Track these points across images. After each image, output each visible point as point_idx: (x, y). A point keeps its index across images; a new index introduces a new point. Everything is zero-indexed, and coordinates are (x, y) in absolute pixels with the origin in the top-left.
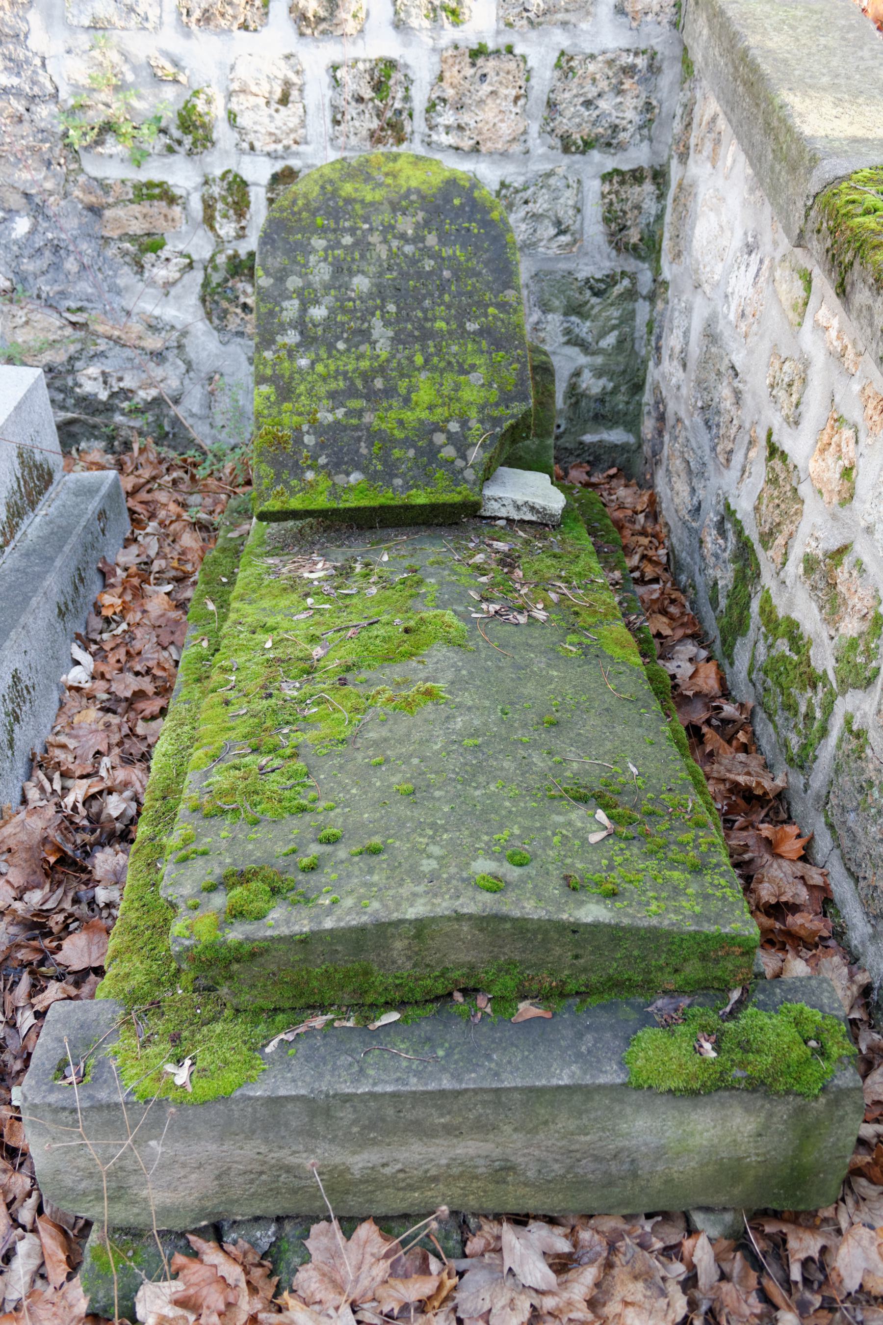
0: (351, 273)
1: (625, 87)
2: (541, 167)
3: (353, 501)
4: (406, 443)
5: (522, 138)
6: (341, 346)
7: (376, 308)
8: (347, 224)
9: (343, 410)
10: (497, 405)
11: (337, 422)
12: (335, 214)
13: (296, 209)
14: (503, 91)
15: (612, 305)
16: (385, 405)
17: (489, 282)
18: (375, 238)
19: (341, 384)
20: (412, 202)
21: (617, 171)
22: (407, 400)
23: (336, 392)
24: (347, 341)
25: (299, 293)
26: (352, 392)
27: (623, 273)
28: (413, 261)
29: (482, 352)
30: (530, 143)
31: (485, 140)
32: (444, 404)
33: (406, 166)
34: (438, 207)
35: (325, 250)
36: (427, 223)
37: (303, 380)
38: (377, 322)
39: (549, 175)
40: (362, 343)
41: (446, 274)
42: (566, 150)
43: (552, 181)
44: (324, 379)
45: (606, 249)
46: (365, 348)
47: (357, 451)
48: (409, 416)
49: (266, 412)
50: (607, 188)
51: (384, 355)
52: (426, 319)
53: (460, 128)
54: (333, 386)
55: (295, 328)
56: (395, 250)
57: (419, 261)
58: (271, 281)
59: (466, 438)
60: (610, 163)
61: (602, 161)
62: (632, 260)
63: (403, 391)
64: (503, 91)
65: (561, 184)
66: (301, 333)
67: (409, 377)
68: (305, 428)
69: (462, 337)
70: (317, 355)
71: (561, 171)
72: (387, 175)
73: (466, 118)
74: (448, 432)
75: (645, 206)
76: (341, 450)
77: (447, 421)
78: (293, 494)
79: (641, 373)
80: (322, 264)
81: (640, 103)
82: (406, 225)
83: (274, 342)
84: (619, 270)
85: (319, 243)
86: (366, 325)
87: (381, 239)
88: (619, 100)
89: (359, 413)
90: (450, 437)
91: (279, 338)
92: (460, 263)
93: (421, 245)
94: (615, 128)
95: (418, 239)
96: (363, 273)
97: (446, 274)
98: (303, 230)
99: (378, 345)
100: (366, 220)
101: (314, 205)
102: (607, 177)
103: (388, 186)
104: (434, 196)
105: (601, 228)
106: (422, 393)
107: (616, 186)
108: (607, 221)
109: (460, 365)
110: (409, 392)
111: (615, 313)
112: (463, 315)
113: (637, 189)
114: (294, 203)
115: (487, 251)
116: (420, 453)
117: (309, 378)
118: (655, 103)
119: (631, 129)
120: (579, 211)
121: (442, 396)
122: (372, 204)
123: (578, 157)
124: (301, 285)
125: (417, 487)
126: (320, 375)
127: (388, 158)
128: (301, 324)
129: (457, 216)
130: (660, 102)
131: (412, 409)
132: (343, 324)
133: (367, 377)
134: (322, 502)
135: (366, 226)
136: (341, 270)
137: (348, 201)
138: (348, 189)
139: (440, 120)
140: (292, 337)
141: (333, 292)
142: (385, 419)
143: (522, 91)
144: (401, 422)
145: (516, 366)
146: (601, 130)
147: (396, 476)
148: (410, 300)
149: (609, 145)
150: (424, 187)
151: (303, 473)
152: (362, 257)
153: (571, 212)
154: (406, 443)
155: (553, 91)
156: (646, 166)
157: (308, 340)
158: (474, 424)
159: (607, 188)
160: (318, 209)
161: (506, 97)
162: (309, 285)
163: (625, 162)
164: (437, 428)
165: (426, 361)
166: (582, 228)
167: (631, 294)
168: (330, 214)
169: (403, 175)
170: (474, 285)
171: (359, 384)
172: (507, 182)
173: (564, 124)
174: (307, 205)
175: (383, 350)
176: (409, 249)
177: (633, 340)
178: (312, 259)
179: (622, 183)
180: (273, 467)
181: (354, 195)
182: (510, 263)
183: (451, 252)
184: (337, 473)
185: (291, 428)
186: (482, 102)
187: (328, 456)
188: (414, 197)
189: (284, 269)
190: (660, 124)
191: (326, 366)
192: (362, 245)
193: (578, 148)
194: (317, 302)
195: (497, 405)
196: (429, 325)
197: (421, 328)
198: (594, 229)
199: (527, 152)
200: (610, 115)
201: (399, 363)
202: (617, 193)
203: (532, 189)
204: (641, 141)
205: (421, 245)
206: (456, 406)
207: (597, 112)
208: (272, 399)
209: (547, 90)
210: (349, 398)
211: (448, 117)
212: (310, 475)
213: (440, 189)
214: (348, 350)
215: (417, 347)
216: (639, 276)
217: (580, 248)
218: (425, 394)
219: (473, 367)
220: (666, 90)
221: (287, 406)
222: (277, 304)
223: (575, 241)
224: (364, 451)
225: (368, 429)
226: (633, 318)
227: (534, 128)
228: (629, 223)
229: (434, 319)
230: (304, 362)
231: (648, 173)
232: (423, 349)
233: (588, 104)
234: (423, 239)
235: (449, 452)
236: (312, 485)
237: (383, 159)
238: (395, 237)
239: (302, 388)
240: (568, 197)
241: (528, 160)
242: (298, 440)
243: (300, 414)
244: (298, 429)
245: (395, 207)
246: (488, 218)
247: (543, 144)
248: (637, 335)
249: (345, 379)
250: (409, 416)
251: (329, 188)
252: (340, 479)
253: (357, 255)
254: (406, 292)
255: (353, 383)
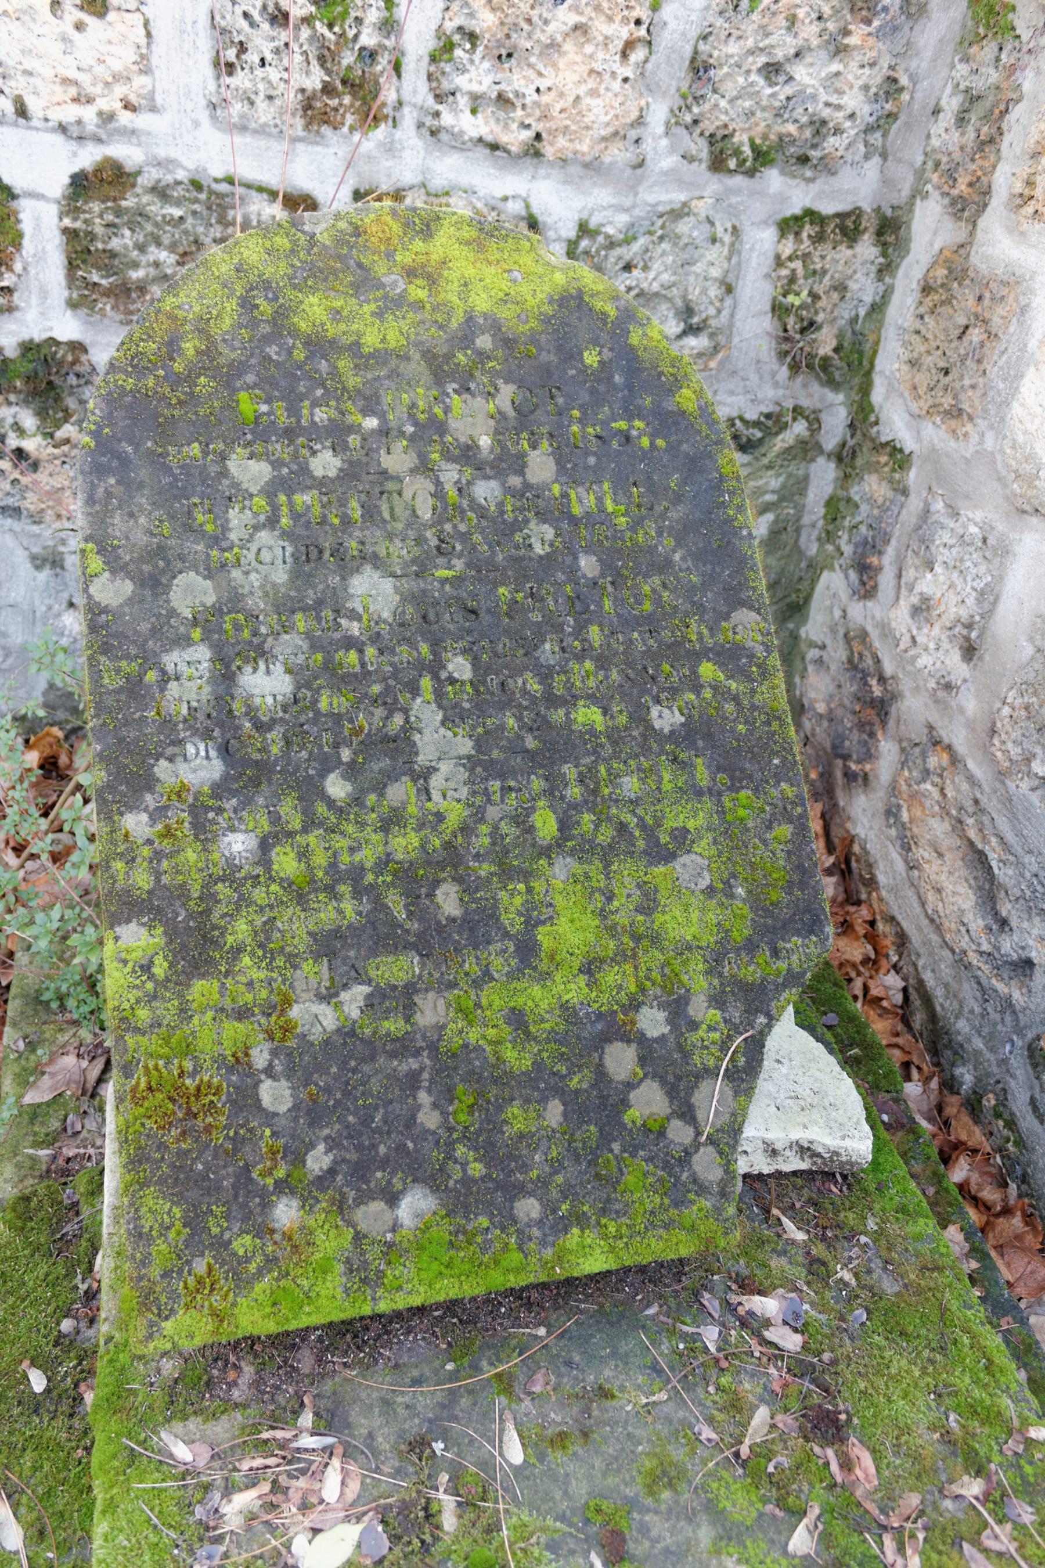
0: (347, 564)
1: (852, 40)
2: (664, 197)
3: (413, 1287)
4: (540, 1084)
5: (633, 134)
6: (337, 787)
7: (421, 667)
8: (321, 415)
9: (361, 990)
10: (750, 947)
11: (348, 1032)
12: (285, 384)
13: (178, 367)
14: (601, 27)
15: (769, 467)
16: (470, 965)
17: (692, 588)
18: (397, 459)
19: (348, 907)
20: (483, 356)
21: (810, 214)
22: (527, 950)
23: (336, 934)
24: (352, 771)
25: (208, 622)
26: (380, 935)
27: (798, 411)
28: (504, 529)
29: (699, 793)
30: (647, 146)
31: (554, 132)
32: (621, 957)
33: (455, 250)
34: (546, 370)
35: (270, 492)
36: (524, 415)
37: (243, 901)
38: (425, 711)
39: (679, 213)
40: (390, 776)
41: (588, 564)
42: (717, 164)
43: (683, 227)
44: (300, 893)
45: (770, 361)
46: (400, 791)
47: (411, 1121)
48: (538, 998)
49: (143, 1014)
50: (788, 248)
51: (455, 814)
52: (551, 700)
53: (502, 100)
54: (327, 915)
55: (206, 735)
56: (452, 493)
57: (516, 526)
58: (128, 587)
59: (686, 1055)
60: (797, 195)
61: (785, 191)
62: (815, 387)
63: (511, 920)
64: (601, 27)
65: (699, 234)
66: (225, 751)
67: (526, 875)
68: (260, 1058)
69: (646, 750)
70: (275, 819)
71: (702, 207)
72: (410, 273)
73: (518, 81)
74: (641, 1039)
75: (853, 286)
76: (366, 1121)
77: (634, 1005)
78: (242, 1282)
79: (804, 585)
80: (264, 536)
81: (875, 78)
82: (473, 420)
83: (149, 782)
84: (789, 404)
85: (250, 471)
86: (398, 720)
87: (410, 460)
88: (835, 67)
89: (404, 998)
90: (649, 1054)
91: (162, 769)
92: (617, 535)
93: (515, 481)
94: (820, 127)
95: (507, 463)
96: (376, 561)
97: (588, 564)
98: (203, 431)
99: (436, 782)
100: (370, 405)
101: (228, 355)
102: (789, 226)
103: (418, 306)
104: (533, 339)
105: (767, 323)
106: (563, 925)
107: (806, 245)
108: (779, 310)
109: (650, 832)
110: (531, 924)
111: (774, 482)
112: (641, 684)
113: (844, 252)
114: (172, 347)
115: (678, 499)
116: (577, 1109)
117: (259, 895)
118: (904, 81)
119: (851, 130)
120: (729, 289)
121: (612, 930)
122: (380, 357)
123: (739, 180)
124: (211, 599)
125: (581, 1220)
126: (288, 884)
127: (407, 225)
128: (222, 721)
129: (598, 400)
130: (914, 79)
131: (544, 977)
132: (337, 718)
133: (415, 879)
134: (330, 1301)
135: (371, 423)
136: (319, 555)
137: (319, 345)
138: (314, 310)
139: (461, 81)
140: (199, 766)
141: (300, 622)
142: (474, 1015)
143: (642, 32)
144: (517, 1019)
145: (784, 831)
146: (791, 128)
147: (520, 1190)
148: (504, 644)
149: (804, 160)
150: (506, 313)
151: (267, 1206)
152: (370, 513)
153: (714, 292)
154: (540, 1084)
155: (705, 38)
156: (867, 208)
157: (245, 776)
158: (700, 1008)
159: (788, 248)
160: (239, 369)
161: (607, 40)
162: (233, 600)
163: (829, 197)
164: (615, 1027)
165: (565, 825)
166: (731, 325)
167: (807, 449)
168: (273, 383)
169: (453, 276)
170: (658, 601)
171: (396, 904)
172: (593, 224)
173: (721, 110)
174: (209, 353)
175: (449, 793)
176: (486, 491)
177: (798, 531)
178: (237, 518)
179: (819, 239)
180: (178, 1198)
181: (332, 330)
182: (736, 532)
183: (591, 500)
184: (359, 1202)
185: (220, 1060)
186: (553, 46)
187: (332, 1144)
188: (484, 342)
189: (161, 551)
190: (907, 125)
191: (303, 854)
192: (362, 475)
193: (742, 163)
194: (258, 653)
195: (750, 947)
196: (558, 715)
197: (540, 726)
198: (753, 327)
199: (641, 164)
200: (814, 97)
201: (495, 834)
202: (806, 257)
203: (642, 241)
204: (867, 157)
205: (515, 481)
206: (651, 958)
207: (788, 90)
208: (160, 969)
209: (694, 33)
210: (373, 952)
211: (477, 75)
212: (286, 1213)
213: (546, 320)
214: (357, 800)
215: (537, 784)
216: (823, 417)
217: (721, 363)
218: (570, 931)
219: (682, 838)
220: (928, 54)
221: (202, 989)
222: (149, 660)
223: (716, 349)
224: (429, 1119)
225: (433, 1047)
226: (803, 492)
227: (659, 114)
228: (820, 318)
229: (570, 701)
230: (239, 844)
231: (870, 223)
232: (553, 790)
233: (772, 70)
234: (519, 465)
235: (648, 1102)
236: (297, 1243)
237: (396, 228)
238: (447, 456)
239: (241, 930)
240: (712, 262)
241: (639, 181)
242: (245, 1099)
243: (242, 1014)
244: (239, 1063)
245: (440, 370)
246: (669, 405)
247: (672, 149)
248: (806, 520)
249: (357, 894)
250: (538, 998)
251: (265, 307)
252: (371, 1215)
253: (355, 509)
254: (490, 611)
255: (380, 905)
